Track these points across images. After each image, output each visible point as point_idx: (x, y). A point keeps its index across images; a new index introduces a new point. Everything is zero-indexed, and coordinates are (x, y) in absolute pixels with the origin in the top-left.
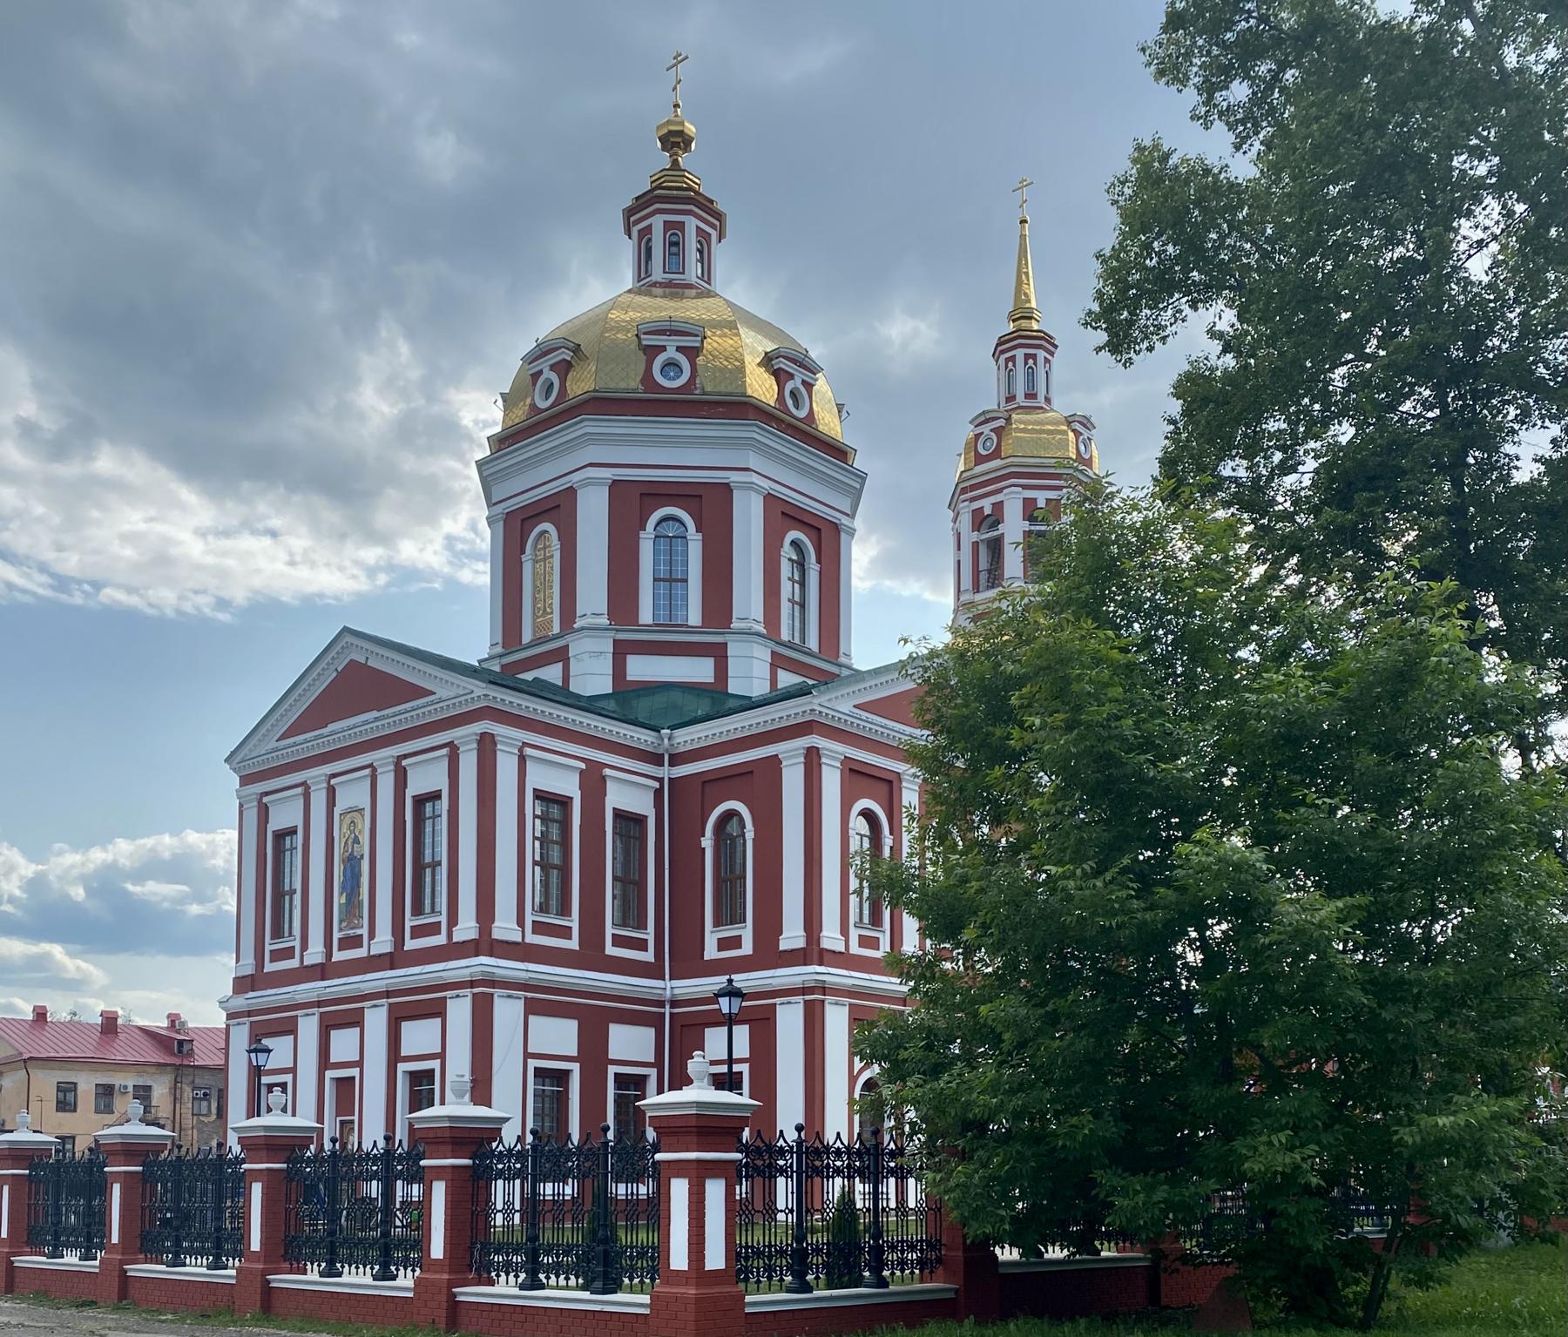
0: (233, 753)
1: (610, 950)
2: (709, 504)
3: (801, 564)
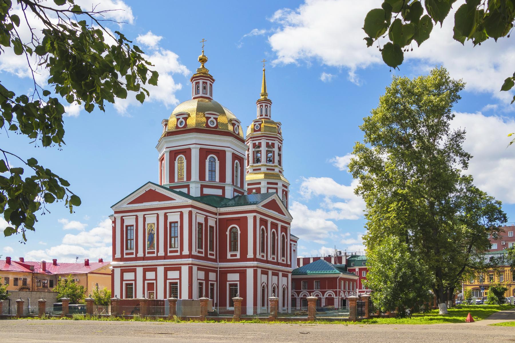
0: (113, 206)
1: (209, 256)
3: (237, 167)
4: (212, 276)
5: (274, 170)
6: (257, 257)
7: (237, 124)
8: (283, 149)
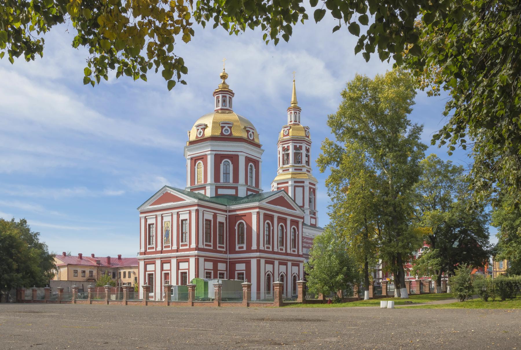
1: (218, 249)
2: (234, 158)
3: (251, 169)
4: (221, 267)
5: (301, 170)
6: (260, 249)
7: (251, 131)
8: (310, 150)
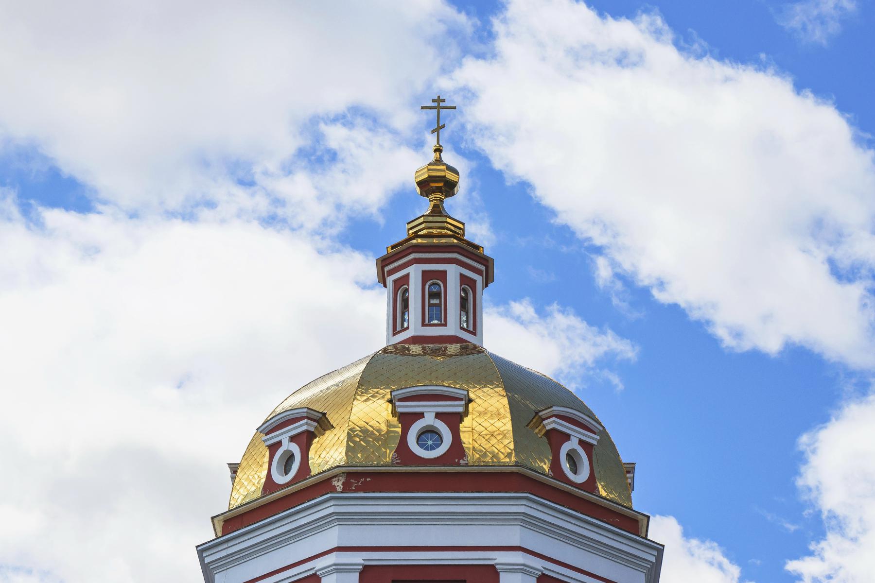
7: (576, 434)
